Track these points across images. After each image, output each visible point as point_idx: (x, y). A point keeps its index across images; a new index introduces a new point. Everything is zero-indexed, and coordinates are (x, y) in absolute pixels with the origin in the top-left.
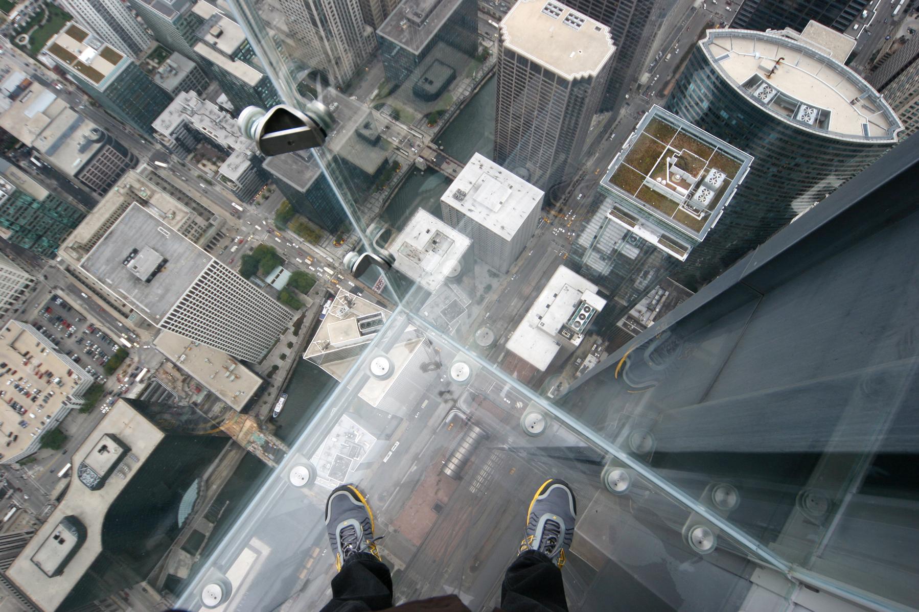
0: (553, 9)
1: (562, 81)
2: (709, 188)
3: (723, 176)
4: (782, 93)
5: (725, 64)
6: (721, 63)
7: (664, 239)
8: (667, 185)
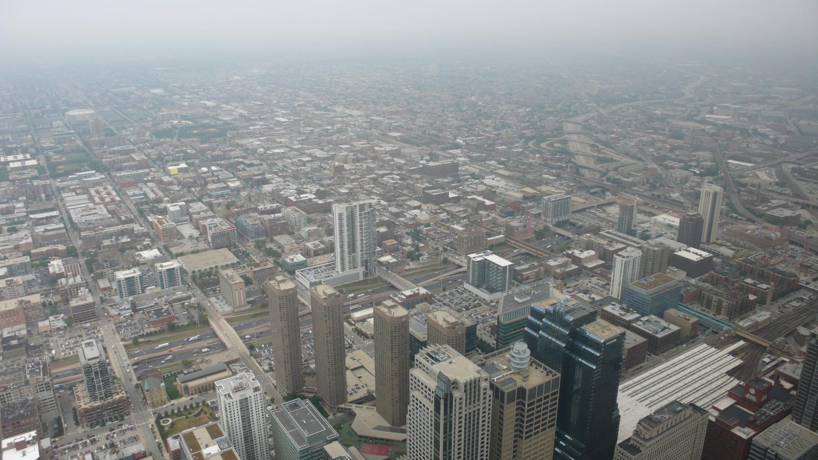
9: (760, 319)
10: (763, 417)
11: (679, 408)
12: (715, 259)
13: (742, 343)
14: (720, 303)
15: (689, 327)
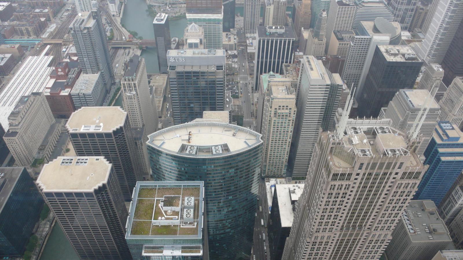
0: (67, 161)
1: (88, 194)
2: (189, 208)
3: (193, 198)
4: (200, 146)
5: (164, 146)
6: (163, 147)
7: (184, 249)
8: (167, 219)
9: (52, 30)
10: (71, 80)
11: (26, 99)
12: (13, 5)
13: (48, 46)
14: (27, 30)
15: (17, 51)
